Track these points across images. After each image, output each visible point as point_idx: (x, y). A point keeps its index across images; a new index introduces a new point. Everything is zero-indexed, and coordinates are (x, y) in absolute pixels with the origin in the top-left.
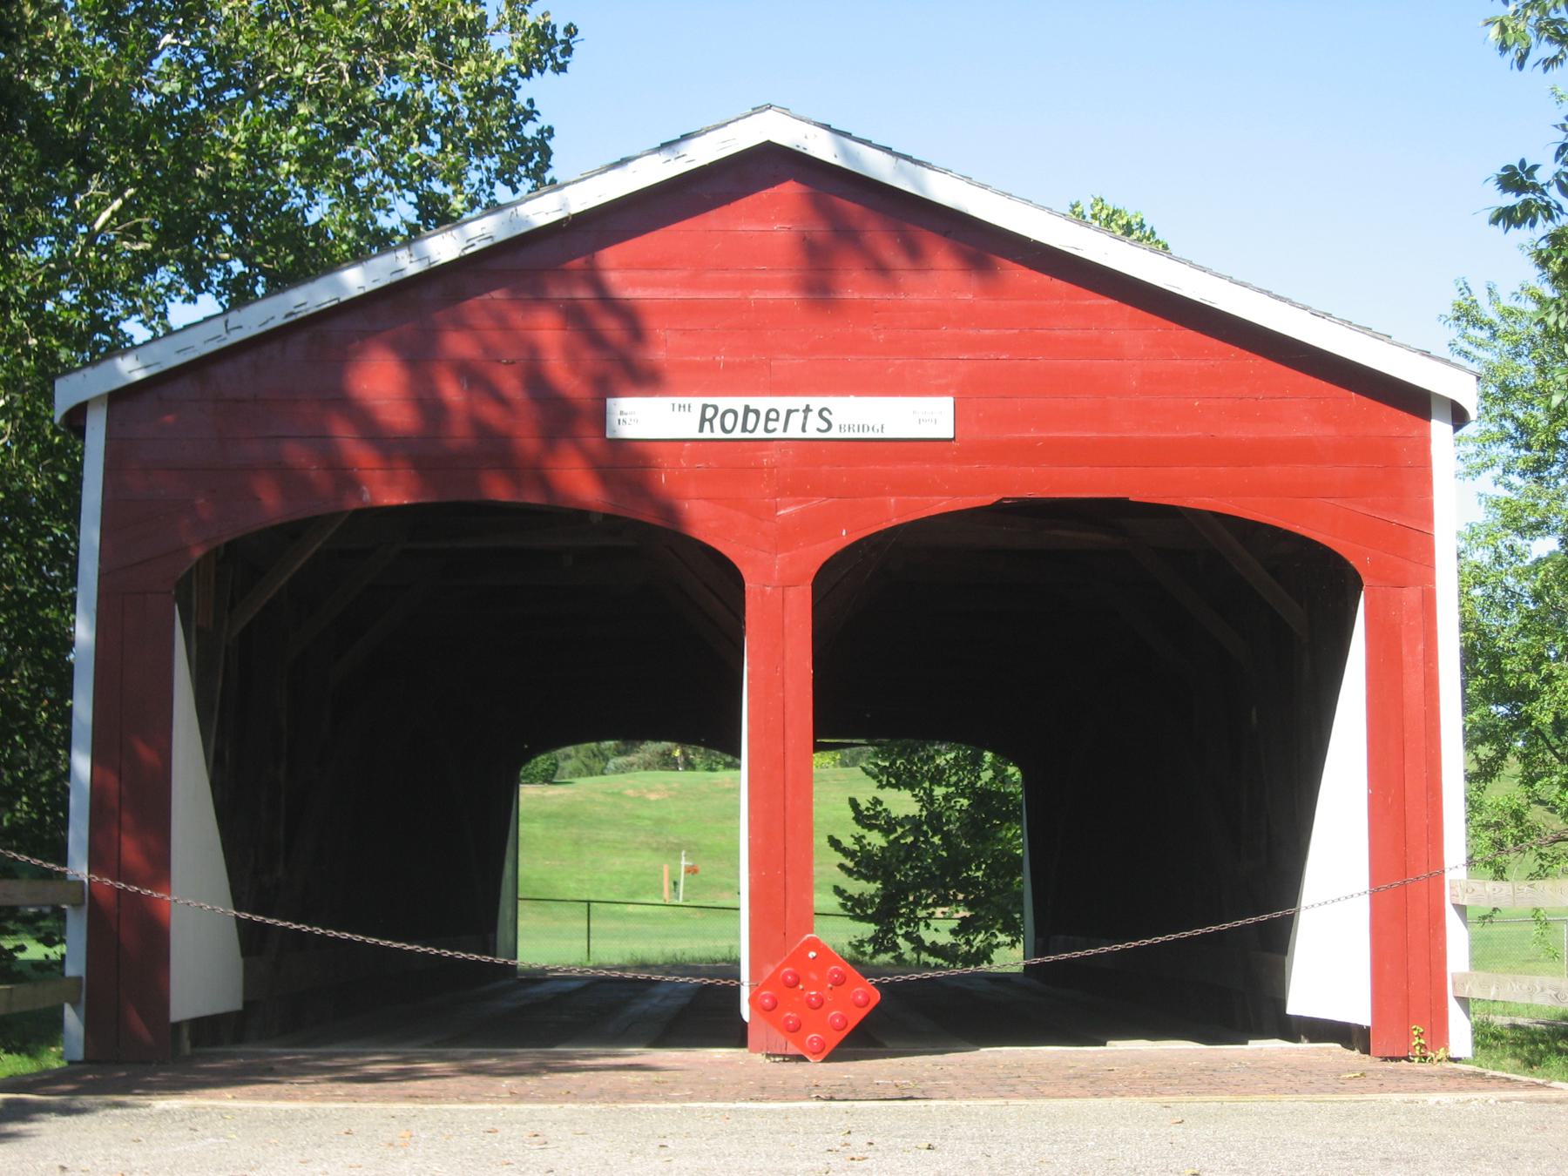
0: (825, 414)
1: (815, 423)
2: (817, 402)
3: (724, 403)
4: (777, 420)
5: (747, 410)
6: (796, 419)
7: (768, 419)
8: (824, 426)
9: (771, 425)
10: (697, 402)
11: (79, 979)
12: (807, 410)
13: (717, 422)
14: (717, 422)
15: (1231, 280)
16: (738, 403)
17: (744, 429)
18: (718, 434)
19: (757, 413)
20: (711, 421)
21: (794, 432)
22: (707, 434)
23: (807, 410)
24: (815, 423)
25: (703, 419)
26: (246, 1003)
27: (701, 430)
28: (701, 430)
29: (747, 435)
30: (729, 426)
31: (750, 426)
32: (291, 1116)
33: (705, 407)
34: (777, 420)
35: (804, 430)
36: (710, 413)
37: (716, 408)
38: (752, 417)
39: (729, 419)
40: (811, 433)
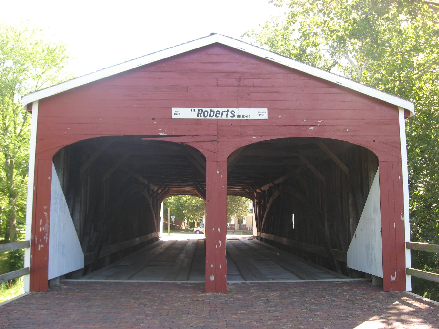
0: (233, 112)
1: (230, 114)
2: (230, 110)
3: (204, 109)
4: (219, 114)
5: (211, 111)
6: (225, 114)
7: (217, 113)
8: (232, 116)
9: (218, 115)
10: (197, 109)
11: (28, 268)
12: (228, 111)
13: (202, 114)
14: (202, 114)
15: (335, 74)
16: (208, 109)
17: (210, 116)
18: (203, 117)
19: (214, 112)
20: (201, 114)
21: (224, 117)
22: (199, 118)
23: (228, 111)
24: (230, 114)
25: (198, 113)
26: (85, 266)
27: (198, 116)
28: (198, 116)
29: (211, 118)
30: (206, 115)
31: (212, 115)
32: (110, 284)
33: (199, 110)
34: (219, 114)
35: (227, 117)
36: (200, 112)
37: (202, 110)
38: (212, 113)
39: (206, 113)
40: (229, 118)
